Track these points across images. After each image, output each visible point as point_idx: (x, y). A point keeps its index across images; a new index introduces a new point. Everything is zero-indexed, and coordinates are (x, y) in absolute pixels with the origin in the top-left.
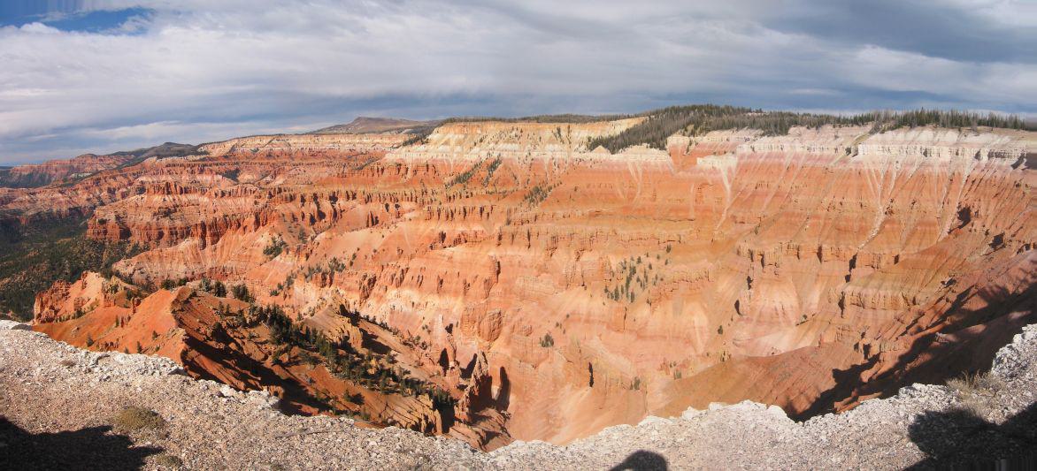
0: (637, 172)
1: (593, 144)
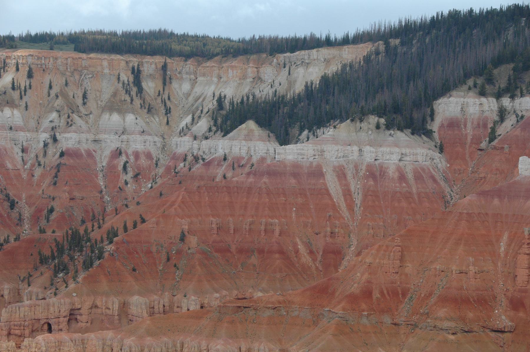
0: (347, 193)
1: (228, 118)
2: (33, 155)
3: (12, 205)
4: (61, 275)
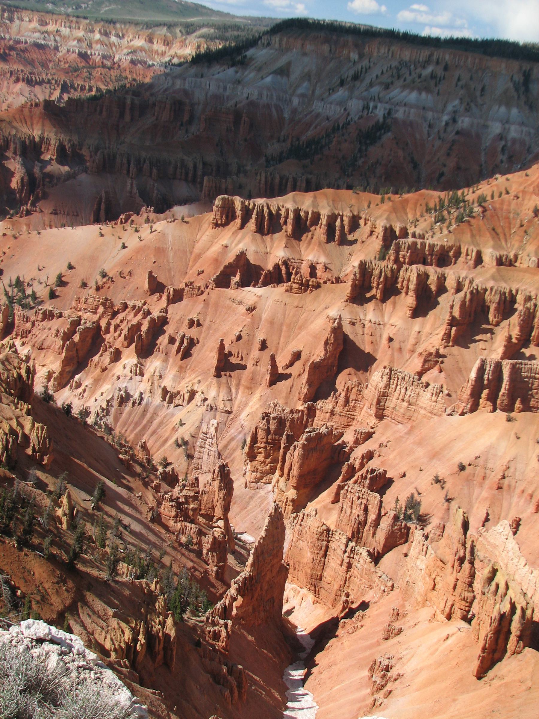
2: (436, 130)
3: (415, 166)
4: (438, 224)
